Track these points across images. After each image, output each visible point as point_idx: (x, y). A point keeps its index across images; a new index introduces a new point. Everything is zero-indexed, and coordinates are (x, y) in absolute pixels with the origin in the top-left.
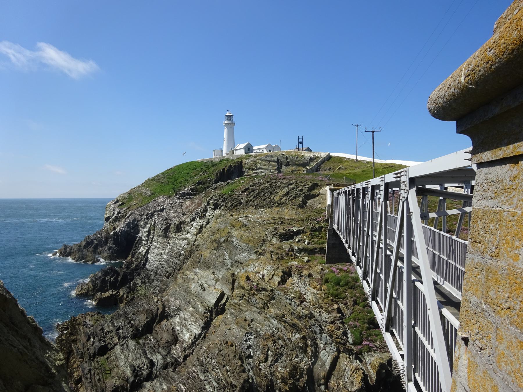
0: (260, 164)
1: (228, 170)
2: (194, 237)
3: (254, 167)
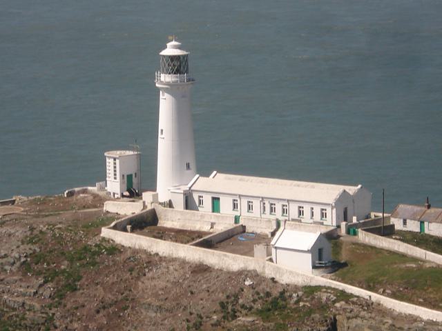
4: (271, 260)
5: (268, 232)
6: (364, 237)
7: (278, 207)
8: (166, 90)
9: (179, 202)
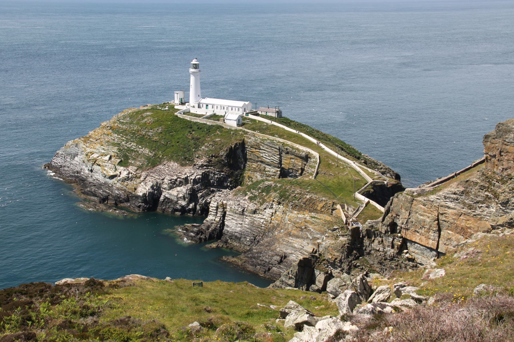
0: (263, 146)
1: (235, 147)
2: (269, 219)
3: (257, 147)
4: (225, 123)
5: (223, 115)
6: (251, 116)
7: (225, 108)
8: (192, 74)
9: (196, 106)
